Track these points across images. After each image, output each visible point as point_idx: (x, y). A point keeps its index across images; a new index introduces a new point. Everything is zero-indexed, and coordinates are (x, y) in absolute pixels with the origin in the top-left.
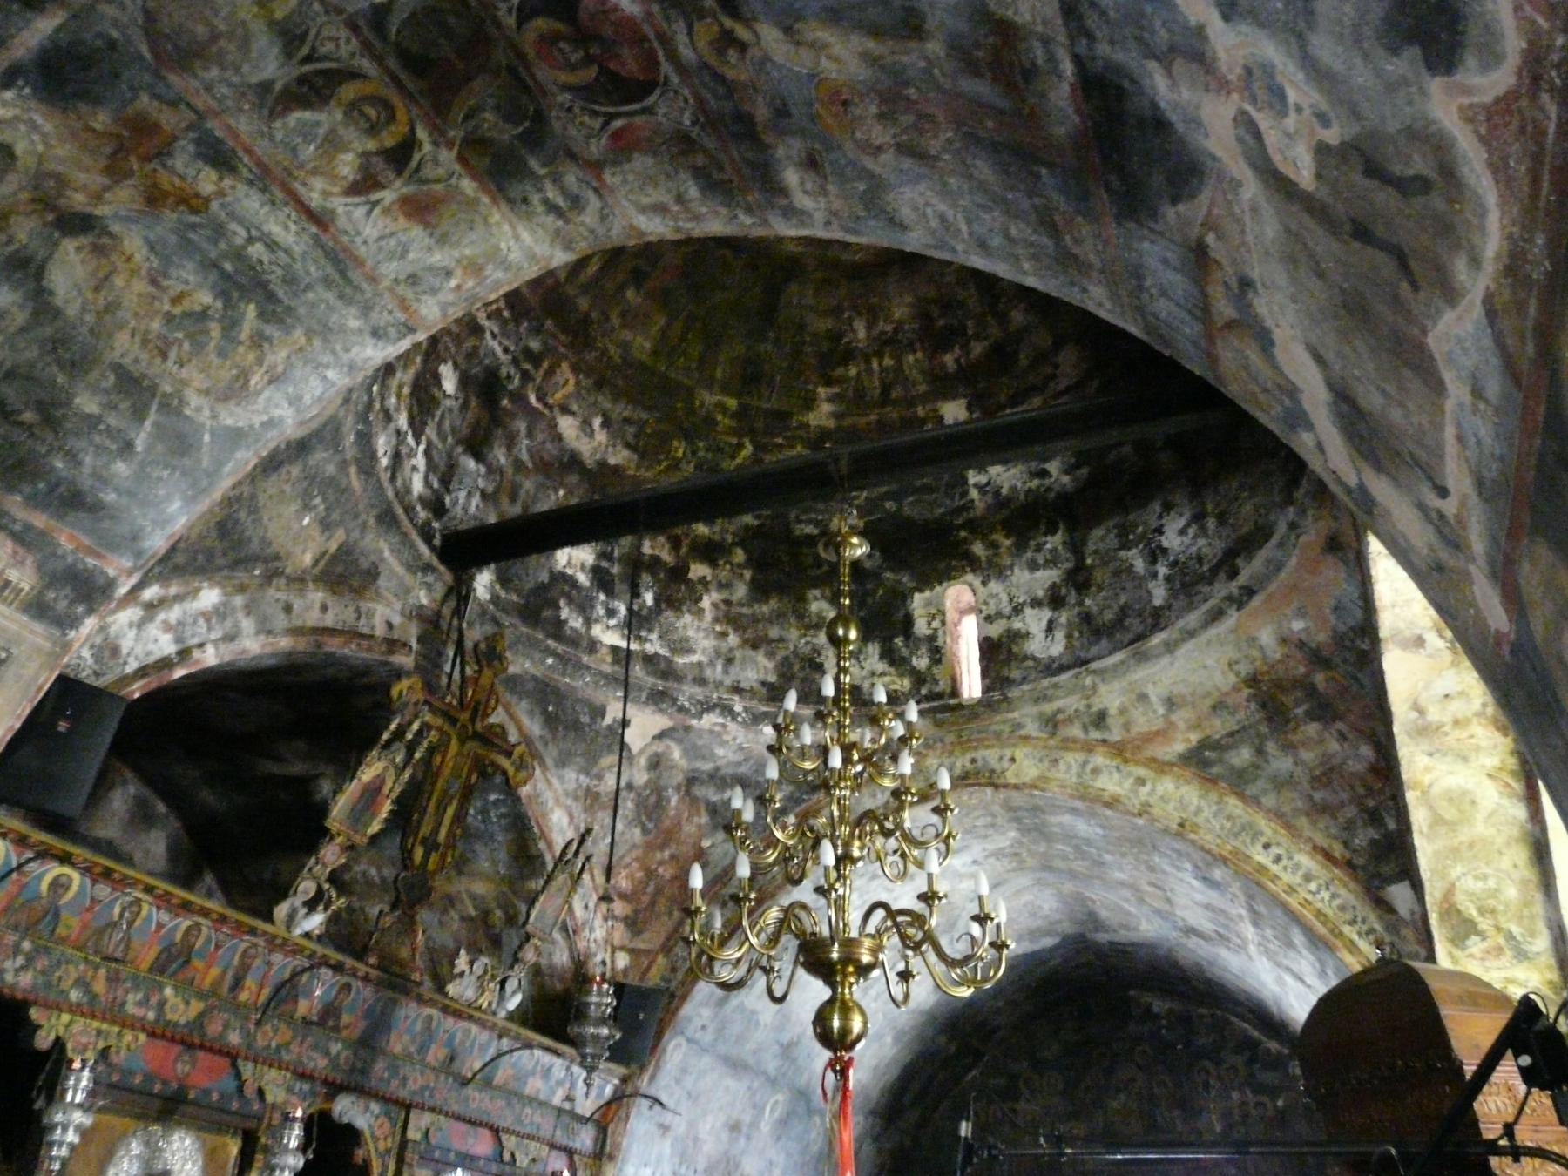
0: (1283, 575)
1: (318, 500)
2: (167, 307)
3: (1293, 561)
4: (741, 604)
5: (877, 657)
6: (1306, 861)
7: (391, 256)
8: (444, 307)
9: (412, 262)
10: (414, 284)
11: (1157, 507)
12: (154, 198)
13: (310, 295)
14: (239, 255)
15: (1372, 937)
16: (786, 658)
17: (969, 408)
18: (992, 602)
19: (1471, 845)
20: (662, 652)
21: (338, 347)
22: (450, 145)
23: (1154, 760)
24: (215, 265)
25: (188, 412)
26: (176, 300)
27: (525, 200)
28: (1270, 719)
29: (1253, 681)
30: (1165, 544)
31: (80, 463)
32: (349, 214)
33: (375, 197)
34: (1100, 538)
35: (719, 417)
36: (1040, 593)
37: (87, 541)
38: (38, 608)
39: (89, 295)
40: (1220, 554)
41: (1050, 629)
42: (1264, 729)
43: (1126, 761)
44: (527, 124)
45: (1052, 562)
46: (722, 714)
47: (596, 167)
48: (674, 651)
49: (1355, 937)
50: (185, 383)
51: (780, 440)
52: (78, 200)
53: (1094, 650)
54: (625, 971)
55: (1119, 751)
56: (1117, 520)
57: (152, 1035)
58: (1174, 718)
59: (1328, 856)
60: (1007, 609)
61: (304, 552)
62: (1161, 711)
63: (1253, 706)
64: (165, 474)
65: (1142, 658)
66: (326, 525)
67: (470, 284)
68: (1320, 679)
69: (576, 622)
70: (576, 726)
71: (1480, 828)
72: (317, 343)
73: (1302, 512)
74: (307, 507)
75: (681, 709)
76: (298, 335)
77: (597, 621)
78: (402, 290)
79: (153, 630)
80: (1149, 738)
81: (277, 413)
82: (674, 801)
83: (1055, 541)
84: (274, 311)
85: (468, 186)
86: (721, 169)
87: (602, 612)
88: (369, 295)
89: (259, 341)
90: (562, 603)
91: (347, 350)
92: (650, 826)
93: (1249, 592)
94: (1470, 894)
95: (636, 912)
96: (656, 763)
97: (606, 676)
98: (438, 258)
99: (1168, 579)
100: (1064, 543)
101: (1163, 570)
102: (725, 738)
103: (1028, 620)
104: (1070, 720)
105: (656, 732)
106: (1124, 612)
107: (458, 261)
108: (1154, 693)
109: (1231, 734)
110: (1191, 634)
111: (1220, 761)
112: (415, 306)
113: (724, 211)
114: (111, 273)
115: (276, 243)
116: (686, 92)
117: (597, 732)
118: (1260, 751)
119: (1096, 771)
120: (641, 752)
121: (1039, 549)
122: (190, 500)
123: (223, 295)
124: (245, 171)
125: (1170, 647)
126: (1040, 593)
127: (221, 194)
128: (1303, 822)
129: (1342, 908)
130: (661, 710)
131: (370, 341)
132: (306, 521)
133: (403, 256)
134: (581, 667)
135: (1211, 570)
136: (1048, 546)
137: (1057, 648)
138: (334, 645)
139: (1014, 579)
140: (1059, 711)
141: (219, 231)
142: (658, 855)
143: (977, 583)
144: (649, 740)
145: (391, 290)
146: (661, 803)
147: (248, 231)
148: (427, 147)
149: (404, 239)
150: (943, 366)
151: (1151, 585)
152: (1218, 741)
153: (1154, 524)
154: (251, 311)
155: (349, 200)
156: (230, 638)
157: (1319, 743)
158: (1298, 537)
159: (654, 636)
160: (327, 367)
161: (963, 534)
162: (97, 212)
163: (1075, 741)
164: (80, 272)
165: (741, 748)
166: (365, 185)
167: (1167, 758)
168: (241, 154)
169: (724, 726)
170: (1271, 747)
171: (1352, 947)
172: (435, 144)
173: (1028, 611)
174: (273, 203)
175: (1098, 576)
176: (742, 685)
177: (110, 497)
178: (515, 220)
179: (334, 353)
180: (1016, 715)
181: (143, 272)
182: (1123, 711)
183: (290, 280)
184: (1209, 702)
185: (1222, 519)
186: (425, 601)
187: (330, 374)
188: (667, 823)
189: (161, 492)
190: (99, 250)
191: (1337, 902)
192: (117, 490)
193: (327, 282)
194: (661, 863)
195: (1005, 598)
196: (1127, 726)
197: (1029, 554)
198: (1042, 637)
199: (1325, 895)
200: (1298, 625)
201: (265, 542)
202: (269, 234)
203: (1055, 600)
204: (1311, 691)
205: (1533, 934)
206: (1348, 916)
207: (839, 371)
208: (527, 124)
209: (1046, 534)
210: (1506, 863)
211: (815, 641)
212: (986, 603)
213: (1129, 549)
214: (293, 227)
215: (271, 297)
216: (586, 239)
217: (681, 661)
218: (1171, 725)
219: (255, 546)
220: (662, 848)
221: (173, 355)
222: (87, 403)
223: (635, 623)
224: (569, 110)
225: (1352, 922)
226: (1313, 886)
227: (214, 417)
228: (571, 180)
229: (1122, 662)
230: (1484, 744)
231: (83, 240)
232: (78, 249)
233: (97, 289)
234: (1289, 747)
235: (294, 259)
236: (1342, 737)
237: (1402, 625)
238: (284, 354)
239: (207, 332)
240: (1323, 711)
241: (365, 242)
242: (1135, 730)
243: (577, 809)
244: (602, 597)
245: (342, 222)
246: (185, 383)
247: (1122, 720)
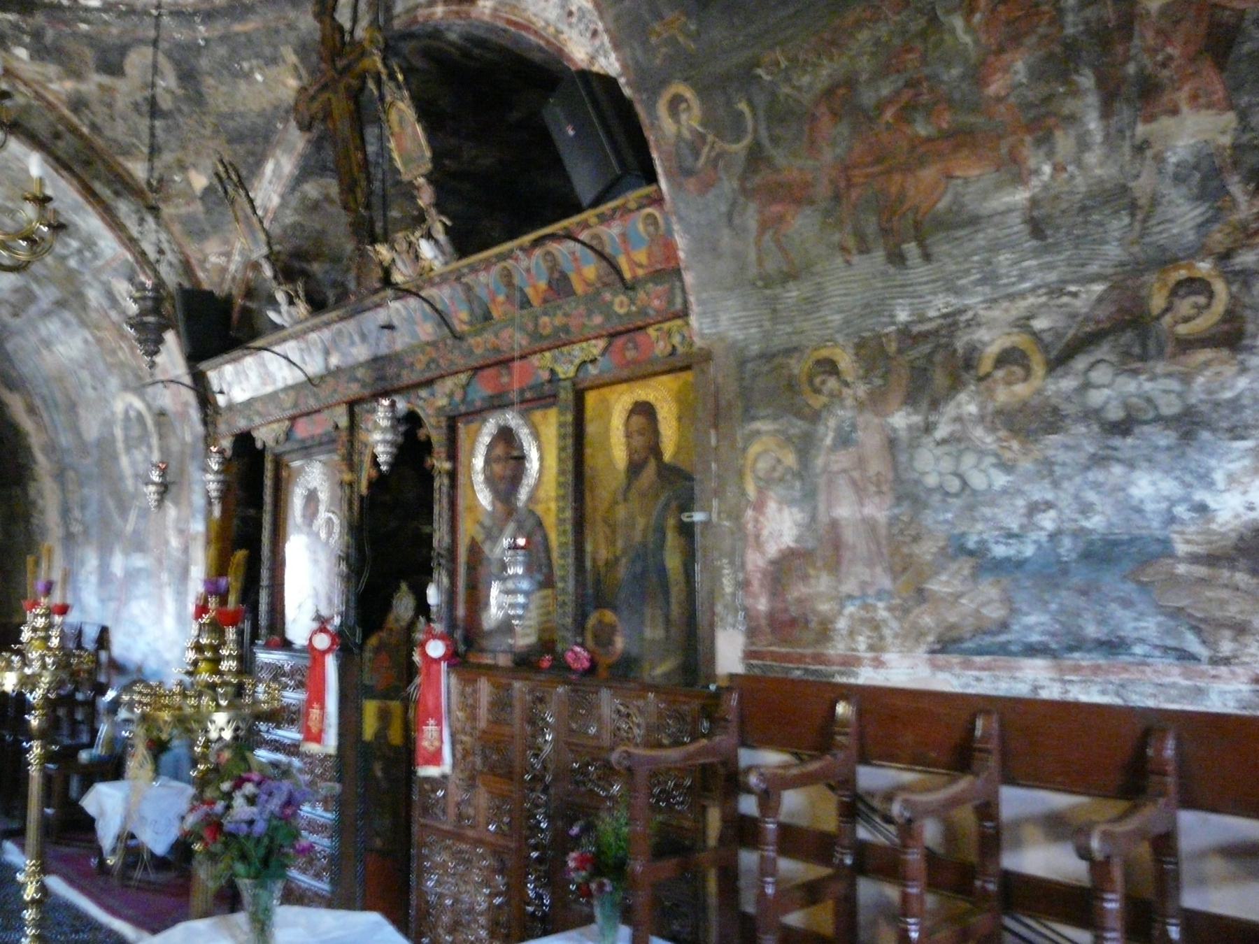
1: (246, 65)
61: (285, 85)
66: (273, 60)
74: (248, 76)
132: (259, 77)
201: (262, 114)
219: (260, 121)
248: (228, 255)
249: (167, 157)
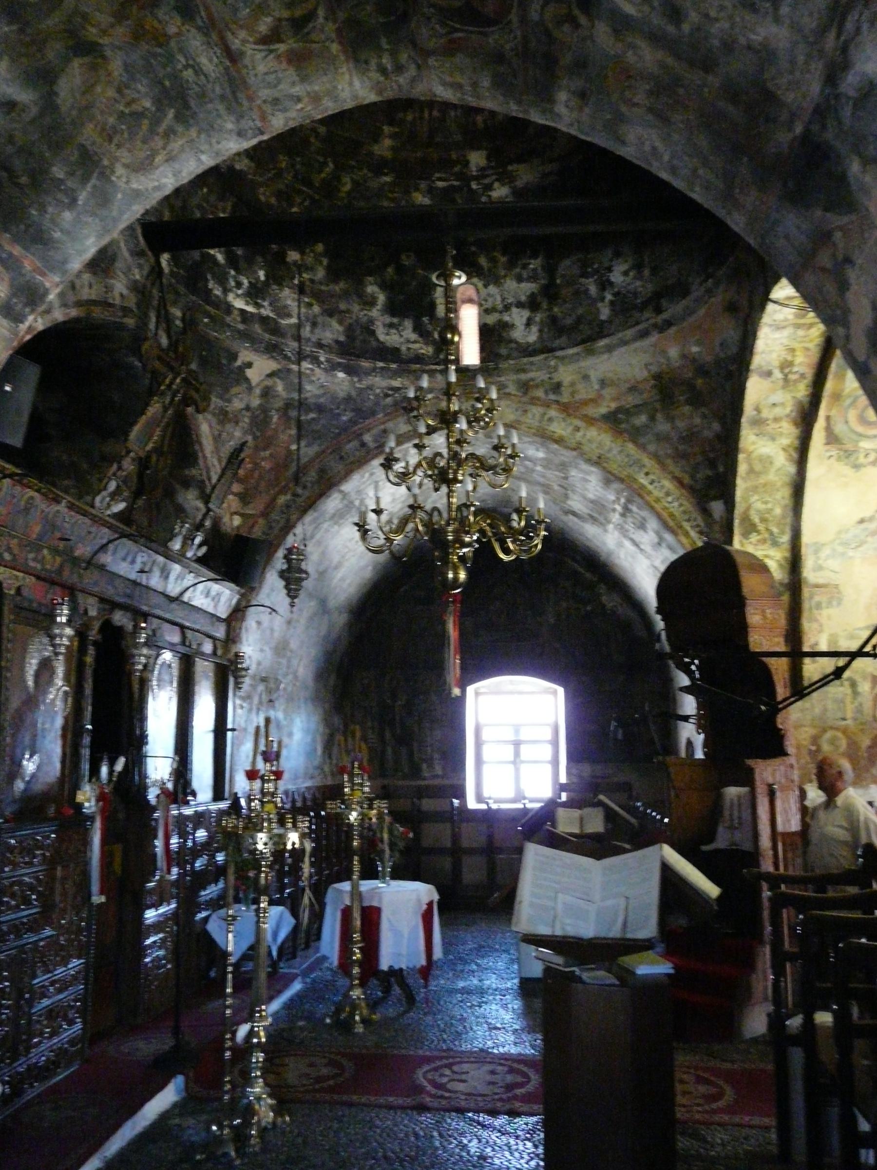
0: (692, 319)
2: (122, 108)
3: (702, 312)
4: (321, 283)
5: (410, 329)
6: (668, 484)
7: (269, 86)
8: (287, 119)
9: (281, 91)
10: (276, 104)
11: (609, 253)
12: (138, 35)
13: (210, 106)
14: (175, 77)
15: (697, 529)
16: (351, 325)
17: (488, 158)
18: (490, 300)
19: (765, 485)
20: (271, 315)
21: (214, 141)
22: (335, 21)
23: (586, 416)
24: (160, 83)
25: (114, 178)
26: (128, 104)
27: (366, 62)
28: (662, 400)
29: (658, 377)
30: (613, 279)
31: (45, 212)
32: (252, 56)
33: (272, 47)
34: (567, 266)
35: (312, 140)
36: (523, 298)
37: (39, 265)
39: (78, 96)
40: (649, 295)
41: (529, 323)
42: (658, 405)
43: (569, 415)
44: (393, 18)
45: (533, 278)
46: (312, 363)
47: (426, 53)
48: (279, 315)
49: (689, 528)
50: (117, 159)
51: (353, 163)
52: (92, 32)
53: (557, 343)
54: (238, 528)
55: (567, 409)
56: (580, 256)
57: (38, 578)
58: (604, 392)
59: (680, 483)
60: (500, 307)
62: (596, 387)
63: (654, 391)
64: (90, 219)
65: (591, 352)
67: (309, 108)
68: (700, 382)
69: (218, 292)
70: (219, 367)
71: (771, 476)
72: (203, 136)
73: (717, 284)
75: (286, 357)
76: (193, 132)
77: (230, 290)
78: (268, 108)
80: (585, 403)
81: (164, 180)
82: (275, 419)
83: (535, 264)
84: (185, 116)
85: (335, 47)
86: (515, 76)
87: (233, 284)
88: (244, 108)
89: (169, 134)
90: (209, 277)
91: (218, 143)
92: (258, 434)
93: (669, 324)
94: (758, 511)
95: (246, 489)
96: (267, 393)
97: (239, 331)
98: (297, 90)
99: (612, 303)
100: (543, 267)
101: (609, 297)
102: (314, 379)
103: (514, 316)
104: (537, 386)
105: (268, 372)
106: (579, 320)
107: (308, 93)
108: (594, 376)
109: (636, 406)
110: (624, 343)
111: (628, 422)
112: (270, 117)
113: (501, 98)
114: (96, 82)
115: (201, 70)
116: (519, 33)
117: (232, 372)
118: (652, 418)
119: (550, 420)
120: (258, 385)
121: (525, 267)
122: (100, 237)
123: (158, 102)
124: (200, 23)
125: (610, 349)
126: (523, 298)
127: (179, 34)
128: (669, 461)
129: (684, 512)
130: (273, 357)
131: (235, 137)
133: (275, 86)
134: (225, 325)
135: (642, 303)
136: (531, 266)
137: (532, 337)
138: (98, 313)
139: (506, 286)
140: (532, 380)
141: (170, 58)
142: (262, 454)
143: (480, 285)
144: (262, 377)
145: (260, 107)
146: (267, 420)
147: (187, 60)
148: (321, 20)
149: (280, 75)
150: (475, 123)
151: (600, 305)
152: (627, 409)
153: (606, 265)
154: (171, 114)
155: (256, 47)
157: (688, 417)
158: (710, 297)
159: (266, 304)
160: (202, 152)
161: (473, 249)
162: (101, 41)
163: (538, 399)
164: (78, 81)
165: (323, 386)
166: (269, 40)
167: (596, 416)
168: (202, 9)
169: (312, 370)
170: (659, 416)
171: (687, 534)
172: (326, 19)
173: (515, 310)
174: (209, 43)
175: (565, 292)
176: (323, 342)
177: (57, 235)
178: (354, 73)
179: (211, 144)
180: (503, 379)
181: (116, 84)
182: (573, 384)
183: (202, 95)
184: (627, 385)
185: (654, 271)
186: (138, 277)
187: (204, 158)
188: (269, 433)
189: (86, 231)
190: (94, 67)
191: (682, 509)
192: (62, 231)
193: (223, 98)
194: (263, 459)
195: (499, 298)
196: (573, 394)
197: (518, 270)
198: (523, 329)
199: (676, 504)
200: (695, 349)
202: (198, 64)
203: (532, 304)
204: (691, 387)
205: (783, 533)
206: (687, 517)
207: (401, 115)
208: (393, 18)
209: (530, 258)
210: (779, 496)
211: (370, 314)
212: (486, 300)
213: (587, 278)
214: (215, 59)
215: (187, 106)
216: (392, 90)
217: (284, 322)
218: (600, 396)
220: (264, 449)
221: (115, 141)
222: (58, 172)
223: (255, 293)
224: (429, 19)
225: (688, 520)
226: (670, 499)
227: (127, 182)
228: (403, 57)
229: (578, 354)
230: (785, 432)
231: (86, 60)
232: (81, 65)
233: (84, 93)
234: (670, 419)
235: (208, 82)
236: (704, 416)
237: (763, 363)
238: (180, 143)
239: (140, 126)
240: (696, 400)
241: (256, 75)
242: (578, 397)
244: (233, 272)
245: (247, 61)
246: (117, 159)
247: (570, 390)
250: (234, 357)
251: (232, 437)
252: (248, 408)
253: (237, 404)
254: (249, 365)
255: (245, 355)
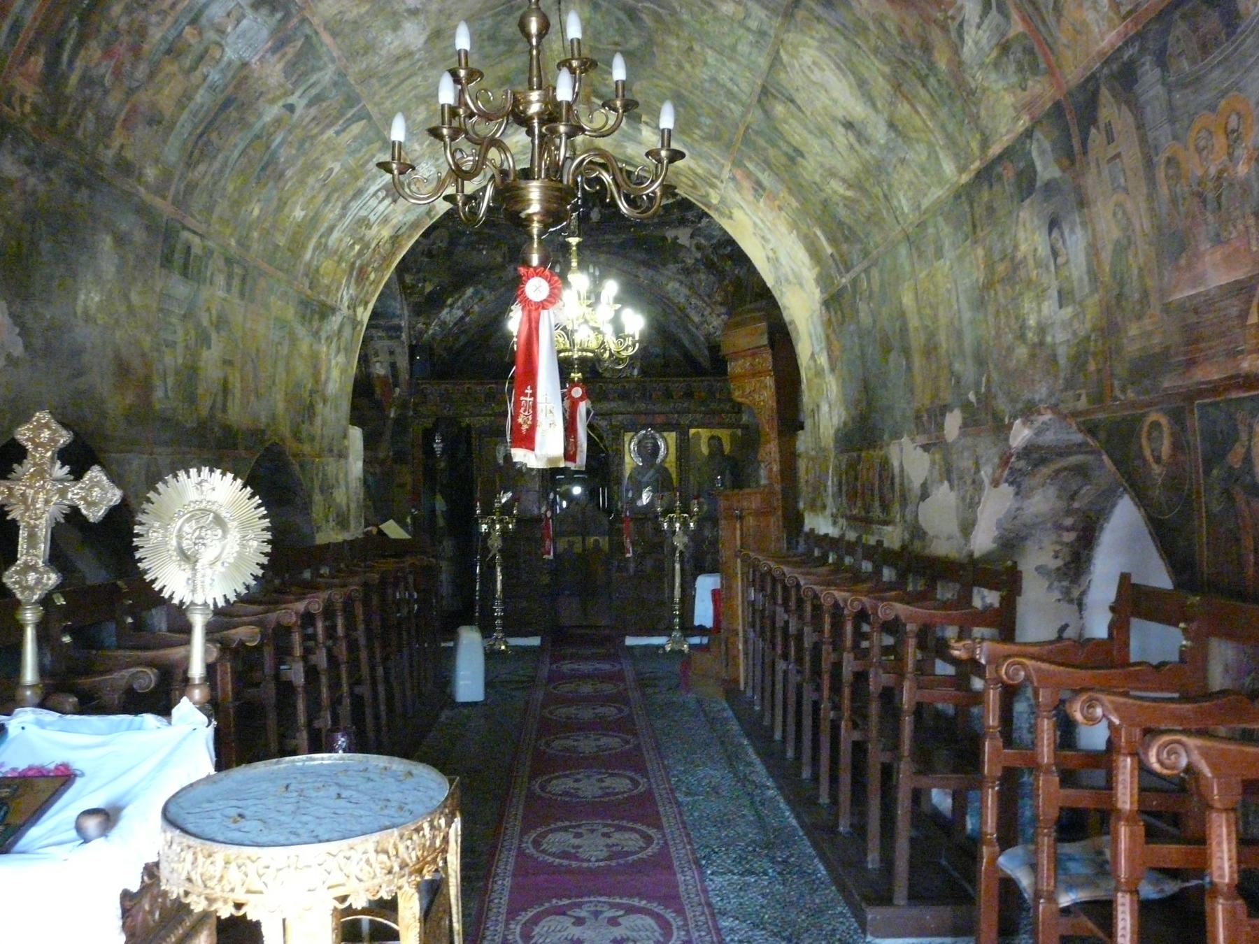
38: (391, 338)
74: (480, 251)
75: (693, 222)
79: (454, 311)
96: (699, 247)
122: (395, 300)
156: (481, 299)
243: (682, 277)
248: (428, 325)
249: (421, 275)
250: (664, 239)
251: (700, 281)
252: (697, 260)
253: (690, 262)
254: (676, 238)
255: (670, 234)
